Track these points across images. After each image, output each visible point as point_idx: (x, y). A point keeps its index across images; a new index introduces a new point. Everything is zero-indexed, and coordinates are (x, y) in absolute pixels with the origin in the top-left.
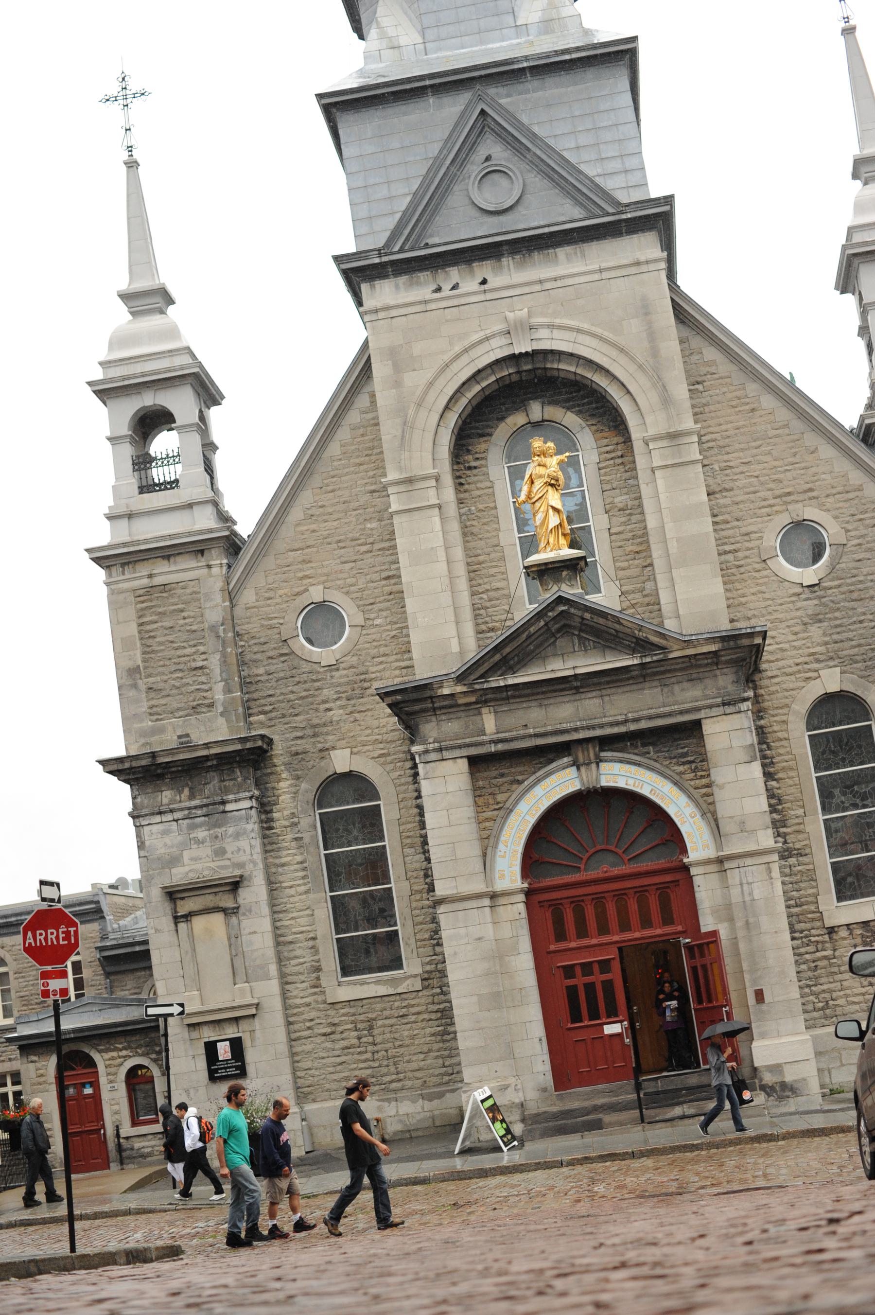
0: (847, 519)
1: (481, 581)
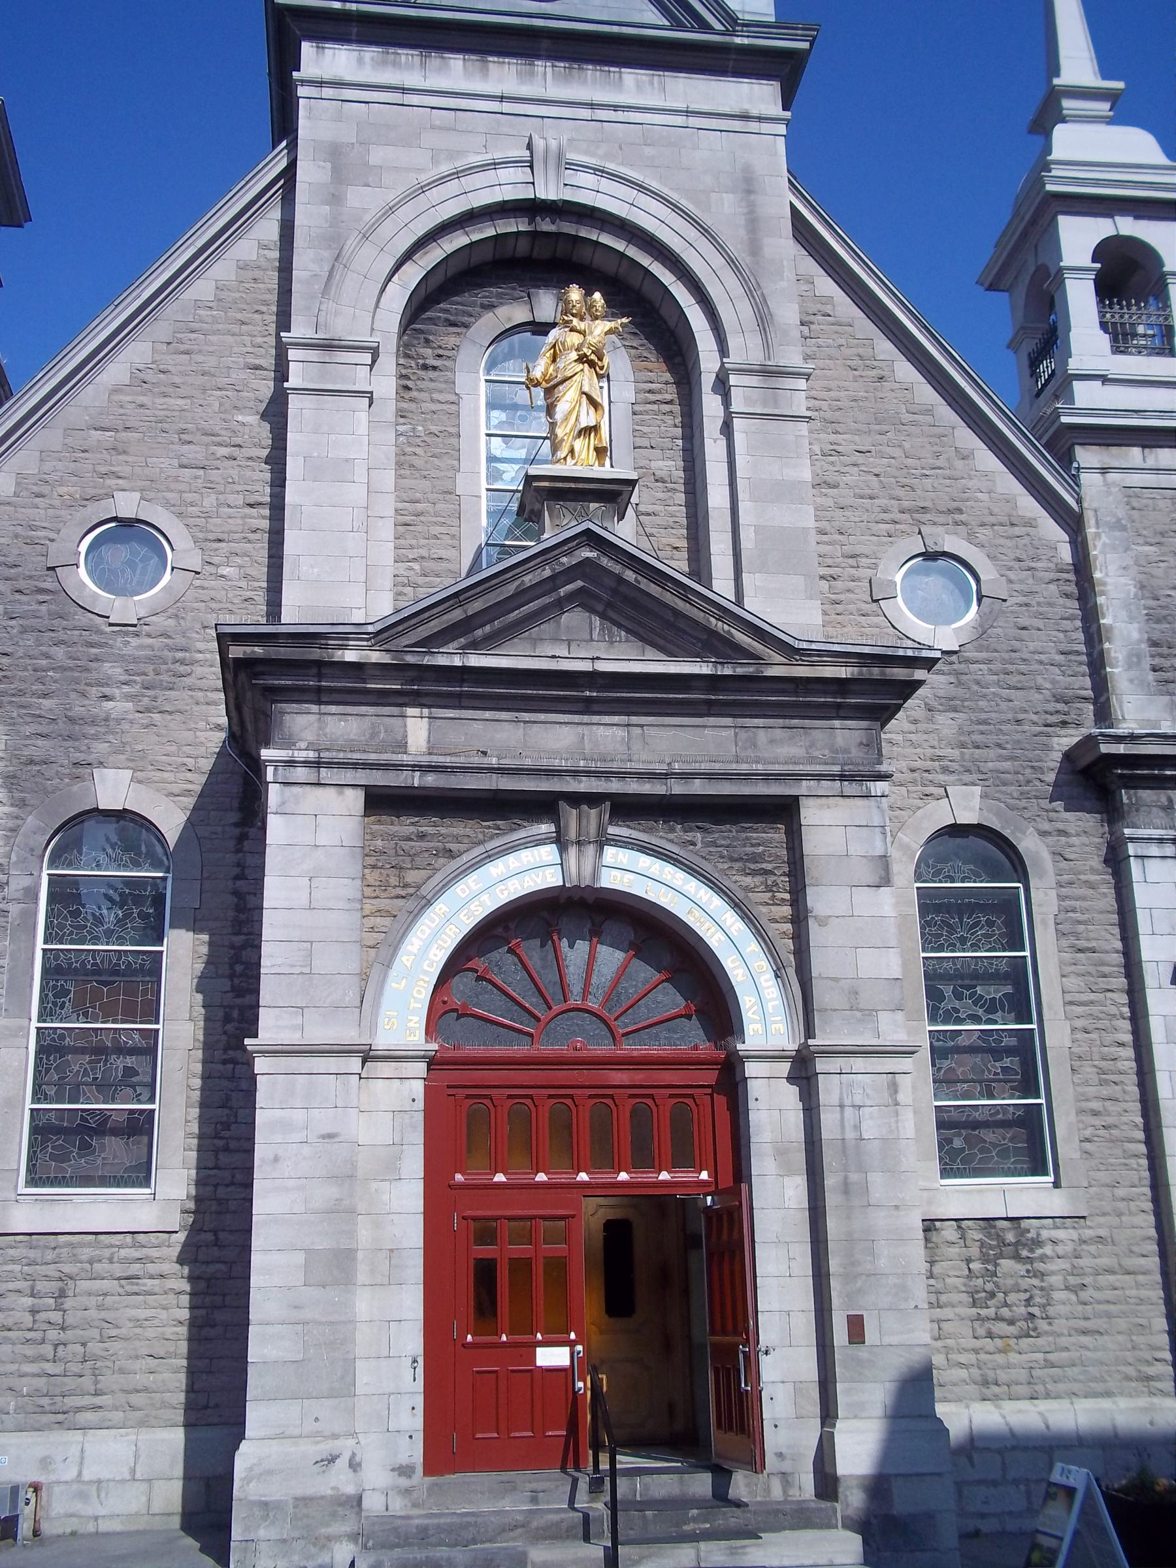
0: (1012, 564)
1: (414, 542)
